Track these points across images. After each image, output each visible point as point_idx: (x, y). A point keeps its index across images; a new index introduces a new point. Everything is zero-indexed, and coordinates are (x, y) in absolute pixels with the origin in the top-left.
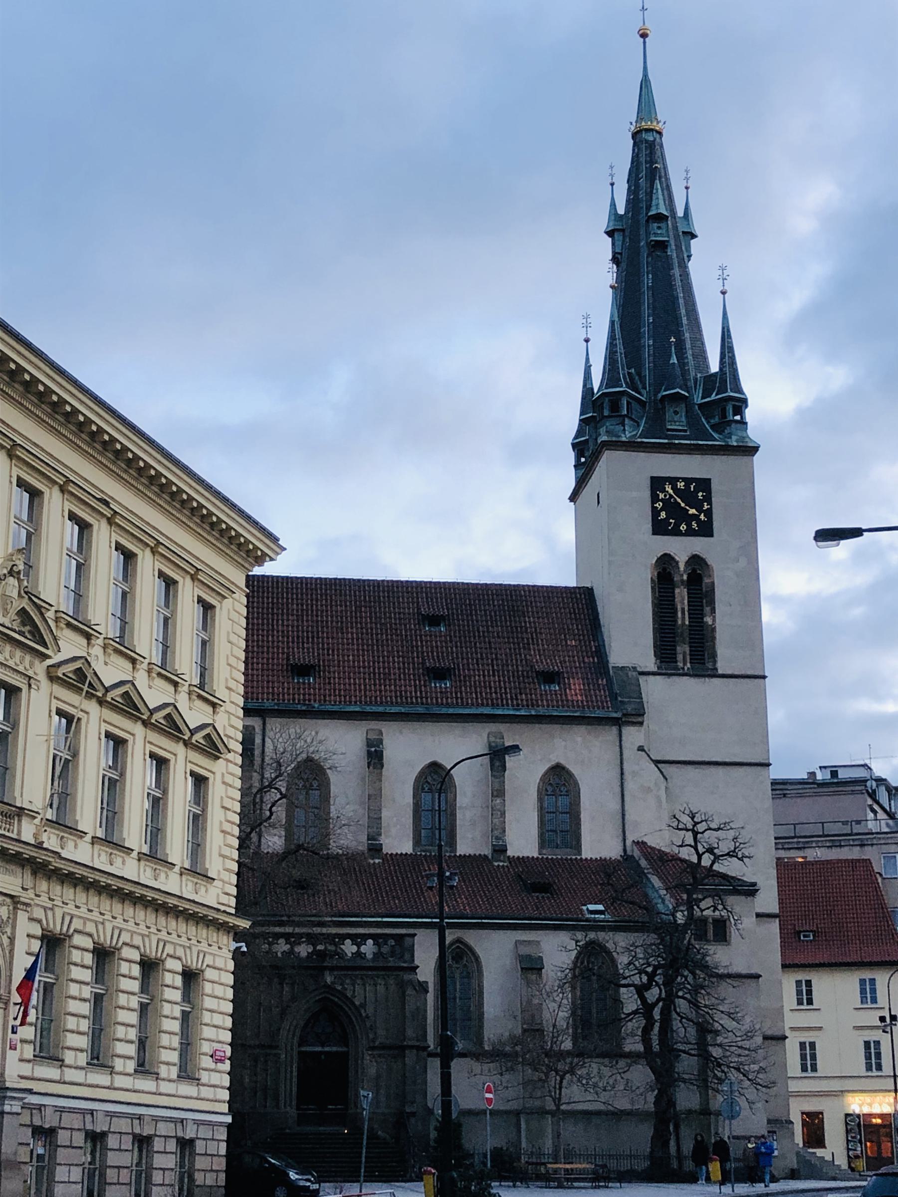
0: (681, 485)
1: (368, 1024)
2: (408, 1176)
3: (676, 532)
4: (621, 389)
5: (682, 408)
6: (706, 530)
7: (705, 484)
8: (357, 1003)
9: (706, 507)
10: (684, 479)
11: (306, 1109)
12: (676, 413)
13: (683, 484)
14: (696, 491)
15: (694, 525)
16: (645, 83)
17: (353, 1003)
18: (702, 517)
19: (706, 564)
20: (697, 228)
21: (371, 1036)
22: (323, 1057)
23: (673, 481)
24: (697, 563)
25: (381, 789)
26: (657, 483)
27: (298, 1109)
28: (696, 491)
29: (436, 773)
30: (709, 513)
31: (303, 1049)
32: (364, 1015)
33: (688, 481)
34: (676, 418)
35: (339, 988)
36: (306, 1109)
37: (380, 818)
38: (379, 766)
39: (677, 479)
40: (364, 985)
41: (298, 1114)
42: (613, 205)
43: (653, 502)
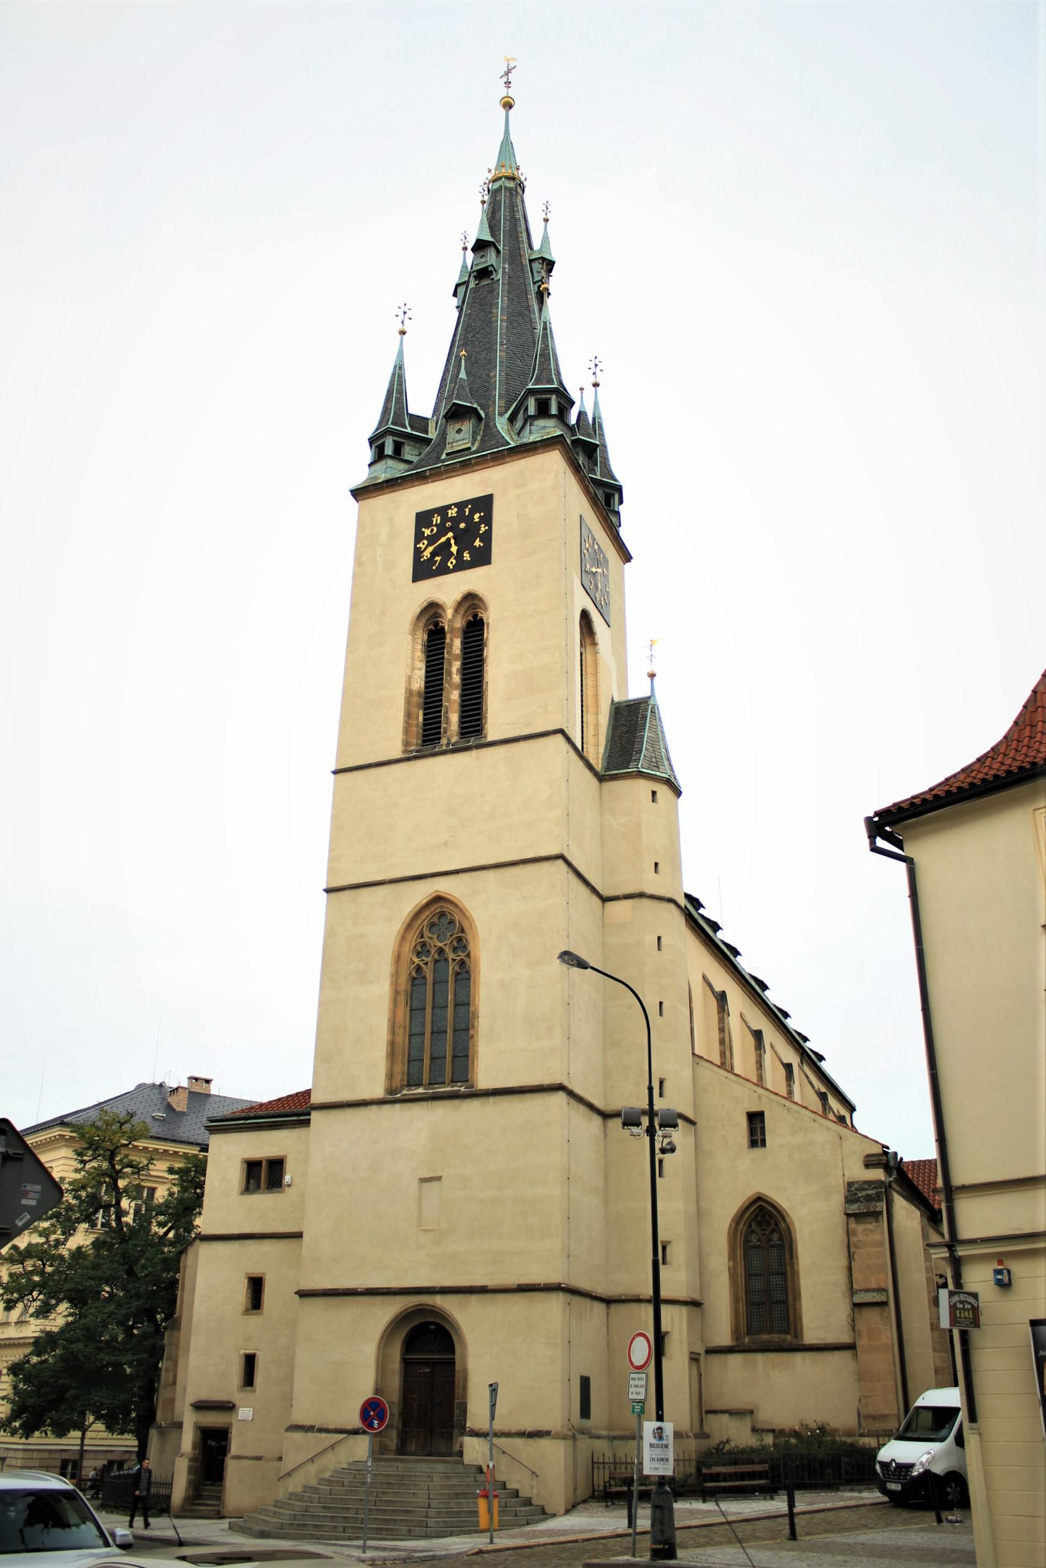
0: (453, 512)
3: (444, 570)
4: (390, 423)
5: (467, 426)
6: (483, 558)
7: (484, 504)
9: (483, 528)
10: (456, 505)
12: (459, 431)
13: (456, 509)
14: (472, 513)
15: (467, 556)
16: (507, 147)
18: (477, 543)
19: (481, 600)
20: (554, 256)
23: (442, 510)
24: (471, 602)
26: (423, 519)
28: (472, 513)
30: (487, 538)
33: (461, 505)
34: (458, 437)
39: (449, 507)
42: (464, 266)
43: (417, 541)
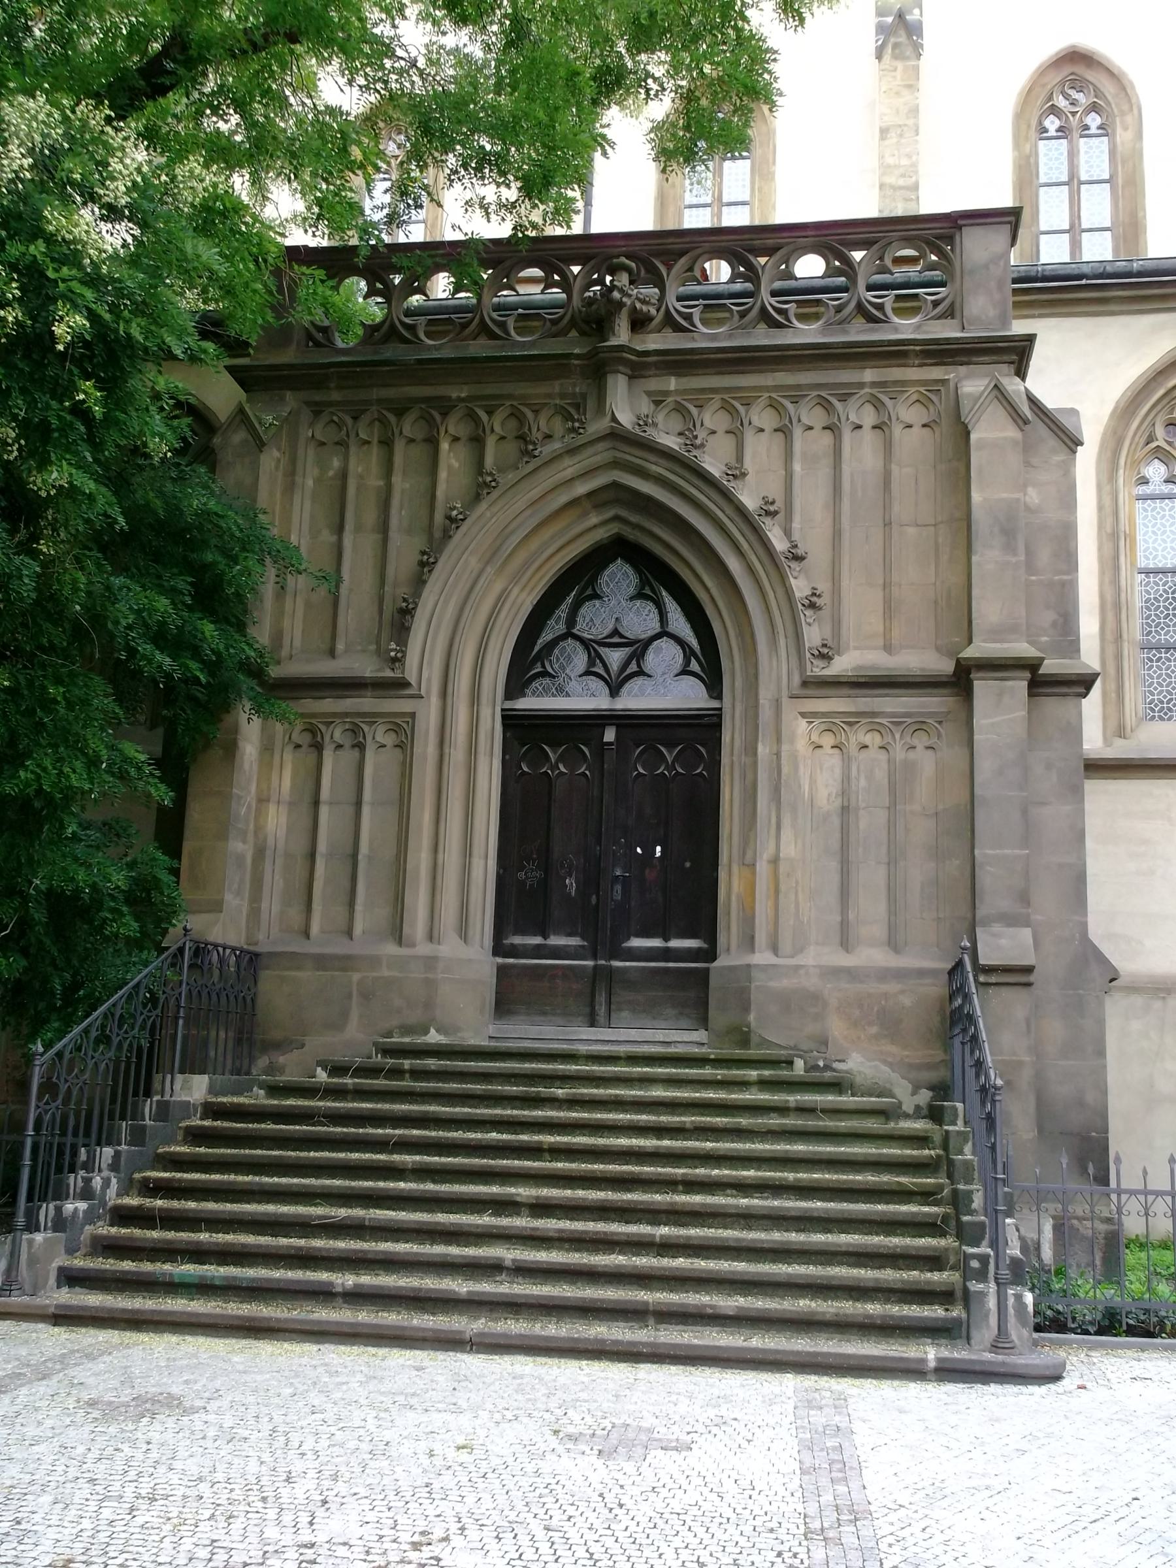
1: (800, 587)
2: (985, 1333)
8: (750, 502)
11: (538, 952)
17: (727, 496)
21: (813, 635)
22: (610, 735)
25: (914, 111)
27: (499, 949)
29: (1078, 84)
31: (527, 703)
32: (779, 544)
35: (671, 442)
36: (538, 952)
37: (915, 187)
38: (909, 52)
40: (784, 431)
41: (502, 971)
